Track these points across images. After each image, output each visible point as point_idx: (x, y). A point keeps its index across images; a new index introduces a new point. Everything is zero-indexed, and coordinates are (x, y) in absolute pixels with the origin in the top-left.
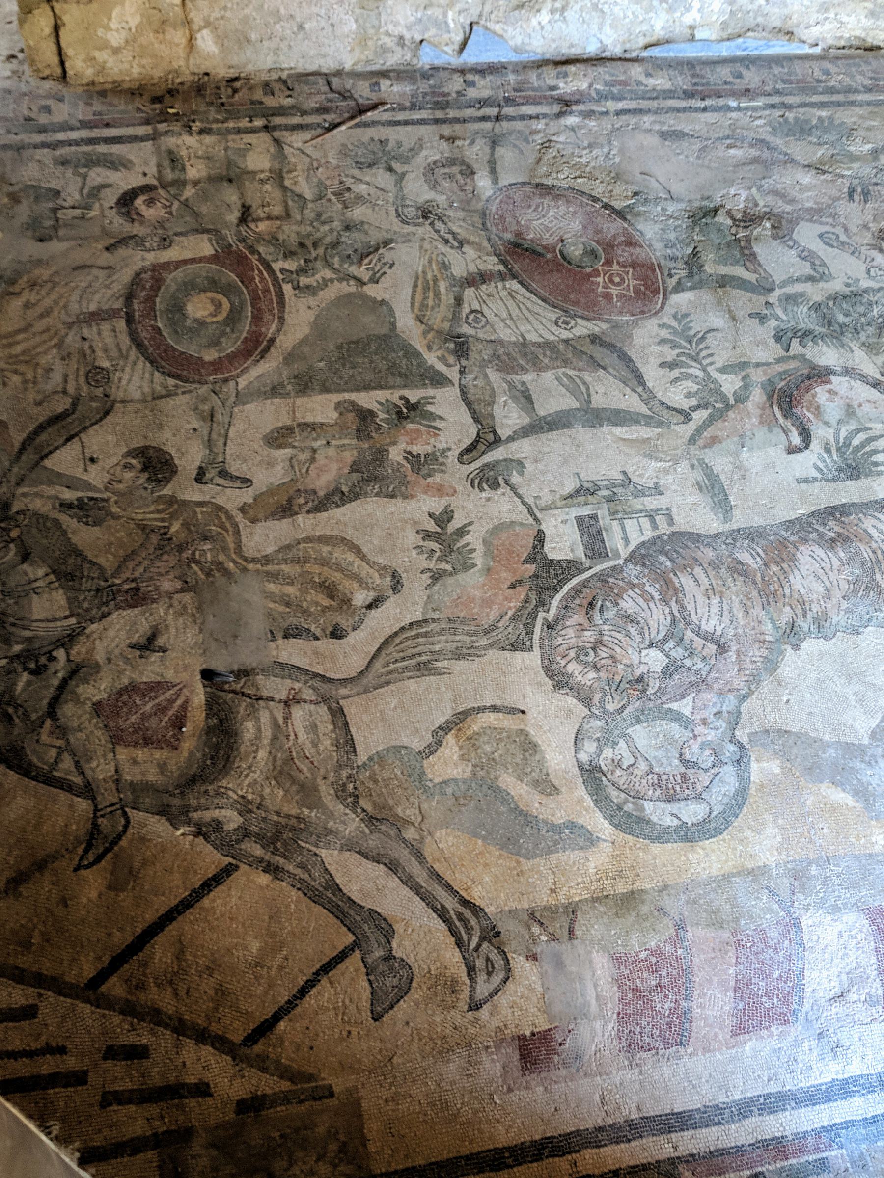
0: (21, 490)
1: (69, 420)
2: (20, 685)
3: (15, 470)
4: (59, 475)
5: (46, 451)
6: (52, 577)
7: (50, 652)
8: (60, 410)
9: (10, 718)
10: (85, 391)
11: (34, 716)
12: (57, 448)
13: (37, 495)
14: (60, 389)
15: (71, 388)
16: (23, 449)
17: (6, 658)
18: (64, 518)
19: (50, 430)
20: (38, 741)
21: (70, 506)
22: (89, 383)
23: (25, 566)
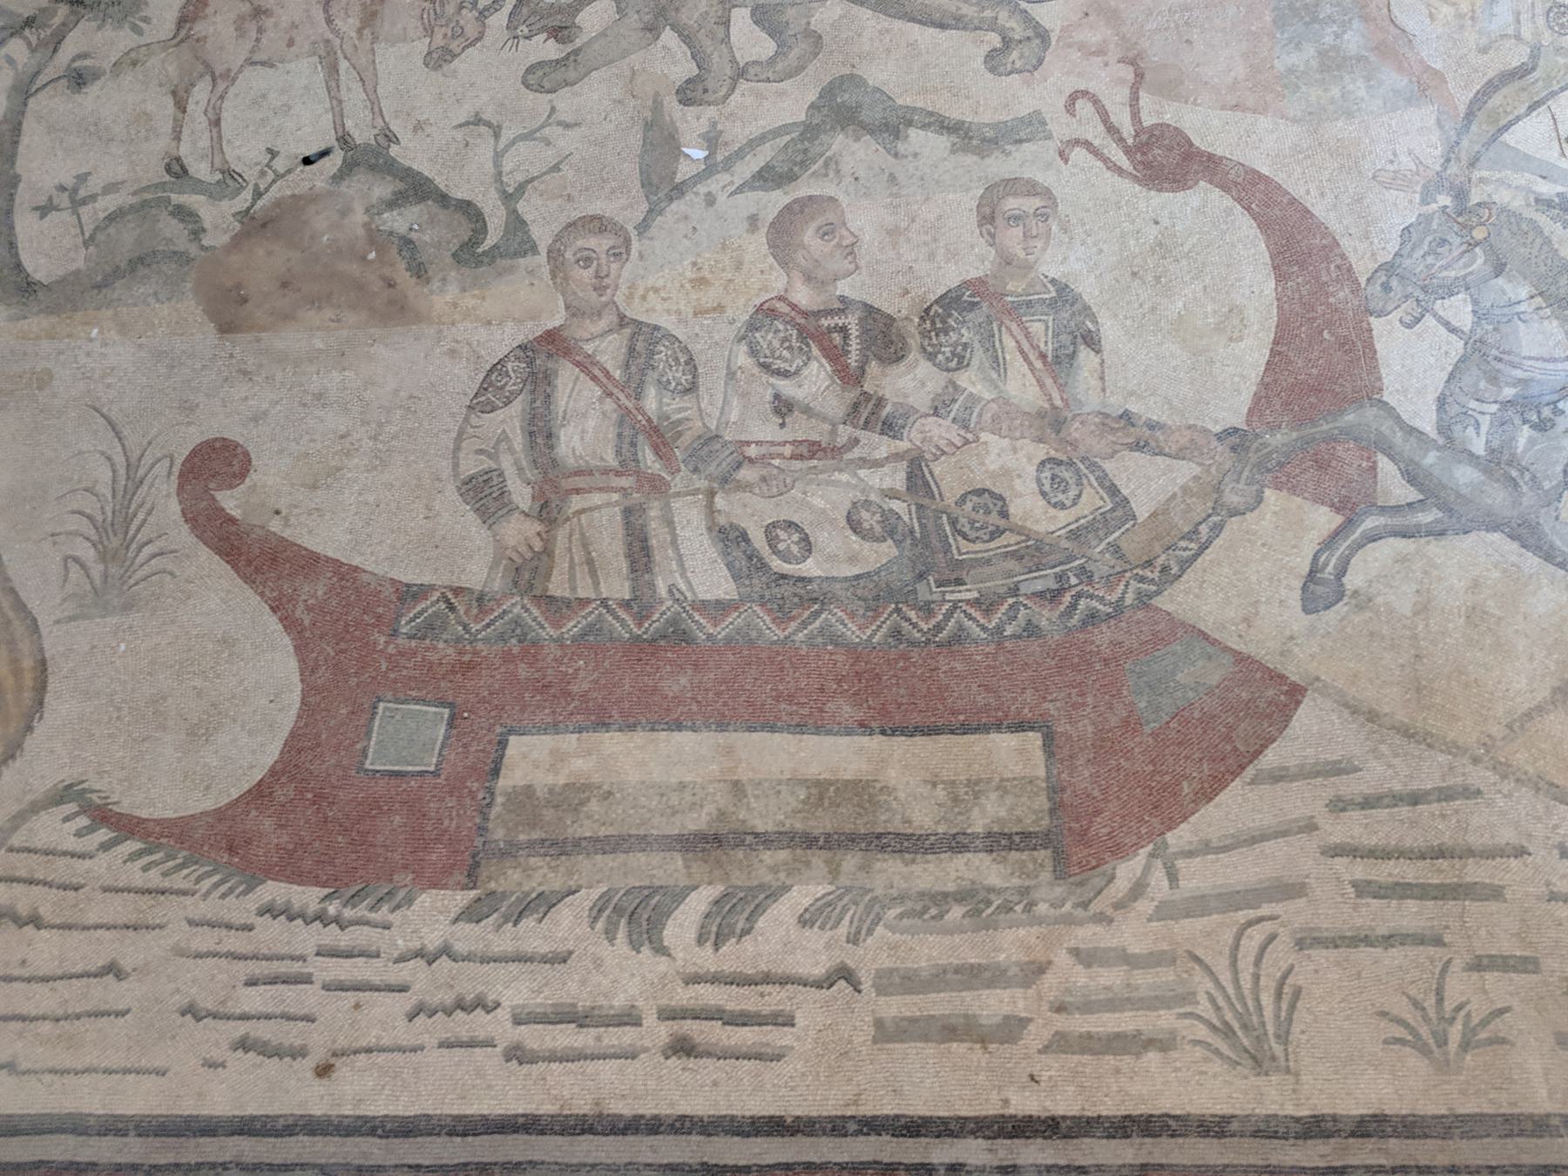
0: (1476, 174)
1: (1531, 78)
2: (1522, 442)
3: (1465, 143)
4: (1527, 157)
5: (1503, 122)
6: (1539, 299)
7: (1555, 403)
8: (1515, 64)
9: (1516, 485)
10: (1547, 38)
11: (1547, 485)
12: (1518, 119)
13: (1501, 182)
14: (1511, 31)
15: (1526, 33)
16: (1470, 115)
17: (1495, 402)
18: (1543, 220)
19: (1505, 91)
20: (1557, 518)
21: (1549, 204)
22: (1551, 28)
23: (1500, 281)
